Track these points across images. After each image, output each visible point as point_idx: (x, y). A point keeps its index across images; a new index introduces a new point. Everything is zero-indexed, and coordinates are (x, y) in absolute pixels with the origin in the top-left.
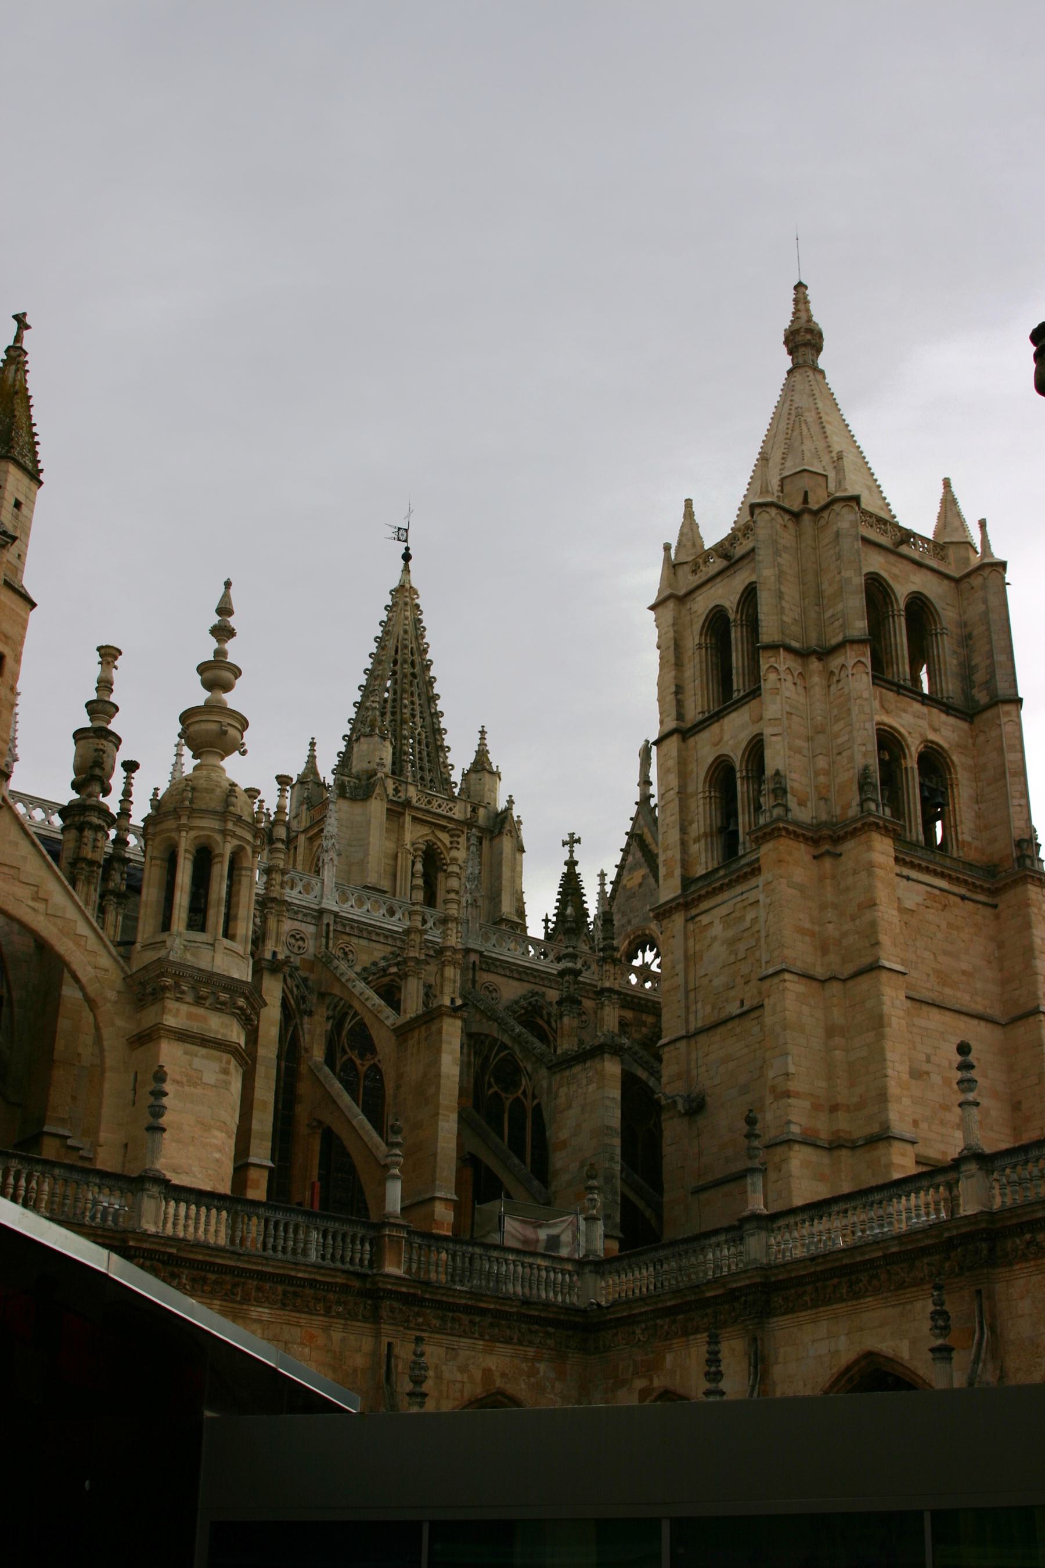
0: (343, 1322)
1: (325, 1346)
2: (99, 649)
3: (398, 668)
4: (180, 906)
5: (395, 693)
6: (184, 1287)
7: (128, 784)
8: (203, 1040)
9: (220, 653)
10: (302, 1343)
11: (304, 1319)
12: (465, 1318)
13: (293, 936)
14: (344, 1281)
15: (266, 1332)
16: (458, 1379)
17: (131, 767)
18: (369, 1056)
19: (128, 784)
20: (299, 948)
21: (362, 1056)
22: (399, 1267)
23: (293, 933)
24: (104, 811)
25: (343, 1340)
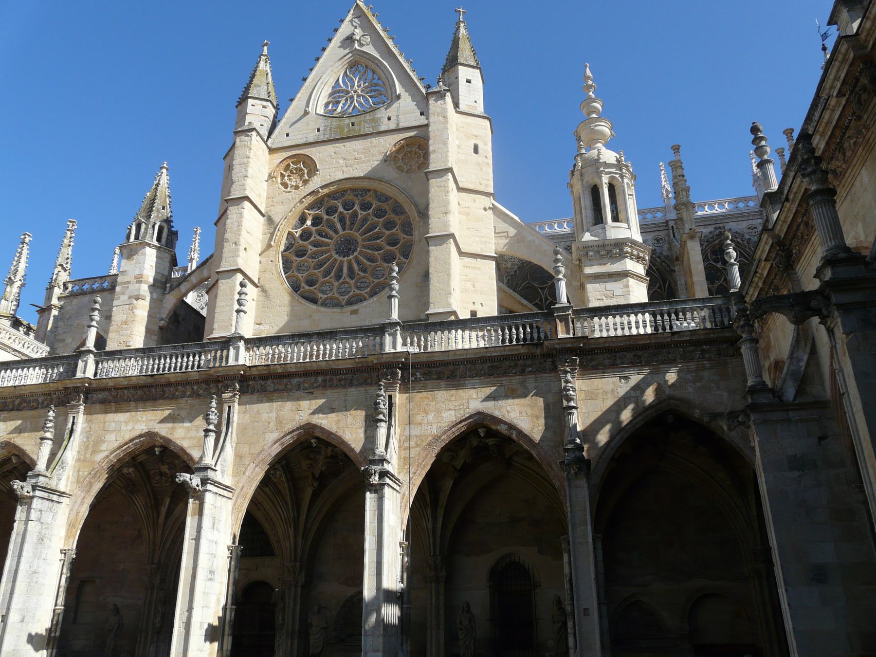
0: (533, 376)
6: (420, 380)
8: (609, 275)
12: (630, 355)
13: (749, 228)
14: (526, 351)
15: (479, 395)
16: (632, 395)
20: (755, 232)
23: (750, 227)
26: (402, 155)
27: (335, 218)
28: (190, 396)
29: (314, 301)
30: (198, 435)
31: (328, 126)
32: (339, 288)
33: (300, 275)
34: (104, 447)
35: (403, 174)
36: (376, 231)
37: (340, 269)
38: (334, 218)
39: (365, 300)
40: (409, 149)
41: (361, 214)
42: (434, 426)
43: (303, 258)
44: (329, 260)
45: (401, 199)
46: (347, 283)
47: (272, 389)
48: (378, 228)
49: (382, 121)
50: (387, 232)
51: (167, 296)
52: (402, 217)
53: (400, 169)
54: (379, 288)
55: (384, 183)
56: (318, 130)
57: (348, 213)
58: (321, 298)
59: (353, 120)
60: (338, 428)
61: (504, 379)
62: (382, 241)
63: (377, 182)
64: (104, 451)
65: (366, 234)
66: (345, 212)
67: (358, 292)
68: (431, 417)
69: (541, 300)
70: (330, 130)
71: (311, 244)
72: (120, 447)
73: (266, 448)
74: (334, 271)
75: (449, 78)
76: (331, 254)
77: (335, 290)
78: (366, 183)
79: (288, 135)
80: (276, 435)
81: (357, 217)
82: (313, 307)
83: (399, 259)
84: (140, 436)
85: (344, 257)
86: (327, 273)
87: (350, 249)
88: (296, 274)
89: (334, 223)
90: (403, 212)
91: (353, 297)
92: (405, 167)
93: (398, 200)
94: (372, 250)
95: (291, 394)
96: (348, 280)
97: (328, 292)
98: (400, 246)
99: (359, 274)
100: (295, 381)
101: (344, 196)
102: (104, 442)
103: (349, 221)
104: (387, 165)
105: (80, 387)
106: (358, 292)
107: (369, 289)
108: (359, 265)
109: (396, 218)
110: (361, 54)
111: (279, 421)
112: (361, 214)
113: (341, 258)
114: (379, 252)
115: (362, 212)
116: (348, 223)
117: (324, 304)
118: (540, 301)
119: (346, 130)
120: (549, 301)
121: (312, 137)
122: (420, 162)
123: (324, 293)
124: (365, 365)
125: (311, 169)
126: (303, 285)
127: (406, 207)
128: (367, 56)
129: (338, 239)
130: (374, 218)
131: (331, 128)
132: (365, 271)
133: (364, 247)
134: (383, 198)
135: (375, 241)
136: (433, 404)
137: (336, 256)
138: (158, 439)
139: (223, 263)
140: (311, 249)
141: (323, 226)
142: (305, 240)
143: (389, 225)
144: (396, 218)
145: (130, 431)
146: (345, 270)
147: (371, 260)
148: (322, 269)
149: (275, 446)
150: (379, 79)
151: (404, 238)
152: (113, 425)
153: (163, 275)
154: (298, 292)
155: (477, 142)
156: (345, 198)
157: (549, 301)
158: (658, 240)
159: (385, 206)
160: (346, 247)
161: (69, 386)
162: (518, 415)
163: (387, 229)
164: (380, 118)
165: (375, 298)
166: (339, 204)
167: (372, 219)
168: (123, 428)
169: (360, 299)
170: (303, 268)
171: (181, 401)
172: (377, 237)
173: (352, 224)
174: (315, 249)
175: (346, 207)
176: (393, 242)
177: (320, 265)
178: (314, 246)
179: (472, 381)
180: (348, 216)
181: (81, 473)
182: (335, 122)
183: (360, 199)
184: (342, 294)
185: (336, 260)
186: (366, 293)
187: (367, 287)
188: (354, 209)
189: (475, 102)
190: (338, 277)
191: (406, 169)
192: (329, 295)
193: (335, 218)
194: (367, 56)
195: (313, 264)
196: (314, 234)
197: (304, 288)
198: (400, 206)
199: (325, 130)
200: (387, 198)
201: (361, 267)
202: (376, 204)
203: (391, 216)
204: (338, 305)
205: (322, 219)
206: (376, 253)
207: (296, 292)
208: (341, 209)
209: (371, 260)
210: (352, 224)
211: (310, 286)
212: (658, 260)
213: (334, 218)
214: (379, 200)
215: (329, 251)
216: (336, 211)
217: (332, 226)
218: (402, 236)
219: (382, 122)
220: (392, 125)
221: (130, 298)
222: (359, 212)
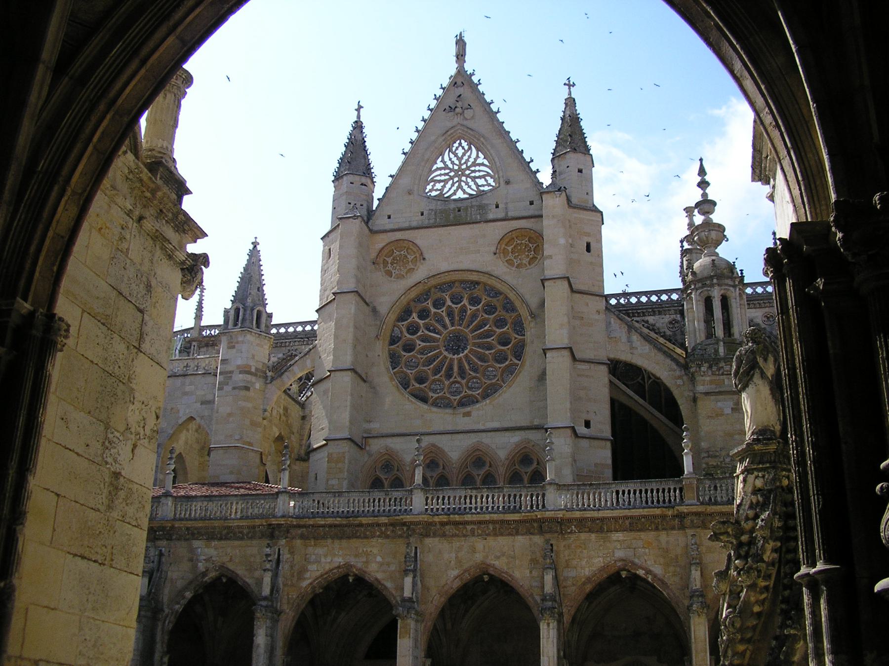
1: (658, 546)
2: (684, 210)
4: (699, 330)
9: (705, 195)
10: (643, 547)
11: (643, 535)
22: (694, 500)
25: (668, 542)
27: (443, 312)
28: (379, 536)
29: (424, 400)
30: (389, 569)
31: (432, 210)
32: (450, 386)
34: (308, 575)
35: (514, 269)
36: (486, 328)
37: (450, 368)
38: (443, 312)
39: (477, 402)
40: (519, 242)
41: (471, 309)
42: (587, 569)
44: (438, 357)
45: (512, 296)
46: (458, 383)
48: (488, 326)
49: (490, 208)
50: (498, 331)
51: (269, 386)
52: (514, 315)
53: (510, 263)
54: (491, 389)
55: (493, 278)
56: (422, 214)
57: (456, 308)
58: (432, 397)
60: (508, 568)
61: (642, 533)
62: (493, 340)
63: (487, 275)
64: (308, 579)
65: (475, 331)
66: (454, 306)
67: (470, 393)
68: (584, 563)
69: (643, 379)
71: (418, 338)
72: (322, 576)
73: (448, 582)
74: (444, 369)
75: (560, 166)
76: (441, 351)
77: (446, 390)
78: (474, 277)
79: (389, 217)
80: (455, 573)
81: (466, 312)
82: (425, 407)
83: (511, 360)
84: (339, 567)
85: (454, 355)
86: (437, 371)
87: (459, 347)
88: (405, 370)
89: (442, 316)
90: (513, 309)
91: (465, 397)
94: (483, 349)
95: (467, 538)
96: (459, 379)
97: (438, 391)
98: (512, 347)
99: (470, 374)
100: (469, 527)
101: (452, 288)
102: (308, 571)
103: (458, 315)
104: (497, 258)
105: (283, 524)
106: (470, 393)
107: (481, 390)
108: (469, 364)
110: (466, 130)
111: (459, 561)
112: (470, 309)
113: (451, 356)
114: (490, 352)
115: (471, 308)
116: (457, 318)
117: (435, 404)
118: (641, 379)
119: (452, 216)
120: (651, 380)
121: (416, 220)
123: (435, 391)
124: (529, 518)
125: (416, 257)
126: (413, 382)
127: (518, 304)
129: (447, 335)
130: (483, 315)
131: (435, 213)
132: (476, 370)
133: (474, 344)
134: (495, 293)
135: (485, 340)
136: (585, 551)
137: (446, 353)
138: (354, 570)
140: (420, 344)
141: (431, 320)
142: (413, 334)
143: (501, 323)
145: (329, 563)
146: (456, 369)
147: (482, 358)
148: (432, 366)
149: (456, 581)
151: (516, 338)
152: (314, 557)
153: (264, 363)
154: (408, 390)
155: (589, 240)
156: (453, 290)
157: (651, 380)
158: (768, 318)
159: (494, 301)
160: (456, 343)
161: (273, 523)
162: (653, 563)
164: (487, 205)
166: (447, 297)
167: (482, 316)
168: (323, 560)
169: (473, 401)
170: (412, 364)
171: (372, 540)
172: (488, 334)
173: (461, 319)
174: (423, 344)
175: (454, 300)
176: (504, 342)
177: (430, 361)
178: (423, 341)
179: (617, 535)
180: (456, 311)
181: (290, 596)
183: (469, 292)
184: (453, 393)
185: (445, 357)
186: (478, 394)
187: (478, 388)
188: (462, 303)
189: (587, 194)
190: (449, 376)
191: (516, 264)
192: (440, 394)
193: (443, 312)
194: (471, 133)
195: (422, 361)
196: (422, 328)
197: (413, 385)
198: (510, 302)
199: (429, 214)
200: (498, 293)
201: (471, 366)
202: (485, 299)
203: (500, 313)
204: (448, 405)
205: (429, 311)
206: (487, 352)
207: (405, 389)
208: (449, 303)
209: (482, 358)
210: (461, 319)
211: (420, 384)
212: (768, 340)
213: (443, 312)
214: (489, 295)
215: (438, 347)
216: (444, 304)
217: (440, 320)
219: (490, 210)
220: (501, 215)
221: (234, 388)
222: (469, 307)
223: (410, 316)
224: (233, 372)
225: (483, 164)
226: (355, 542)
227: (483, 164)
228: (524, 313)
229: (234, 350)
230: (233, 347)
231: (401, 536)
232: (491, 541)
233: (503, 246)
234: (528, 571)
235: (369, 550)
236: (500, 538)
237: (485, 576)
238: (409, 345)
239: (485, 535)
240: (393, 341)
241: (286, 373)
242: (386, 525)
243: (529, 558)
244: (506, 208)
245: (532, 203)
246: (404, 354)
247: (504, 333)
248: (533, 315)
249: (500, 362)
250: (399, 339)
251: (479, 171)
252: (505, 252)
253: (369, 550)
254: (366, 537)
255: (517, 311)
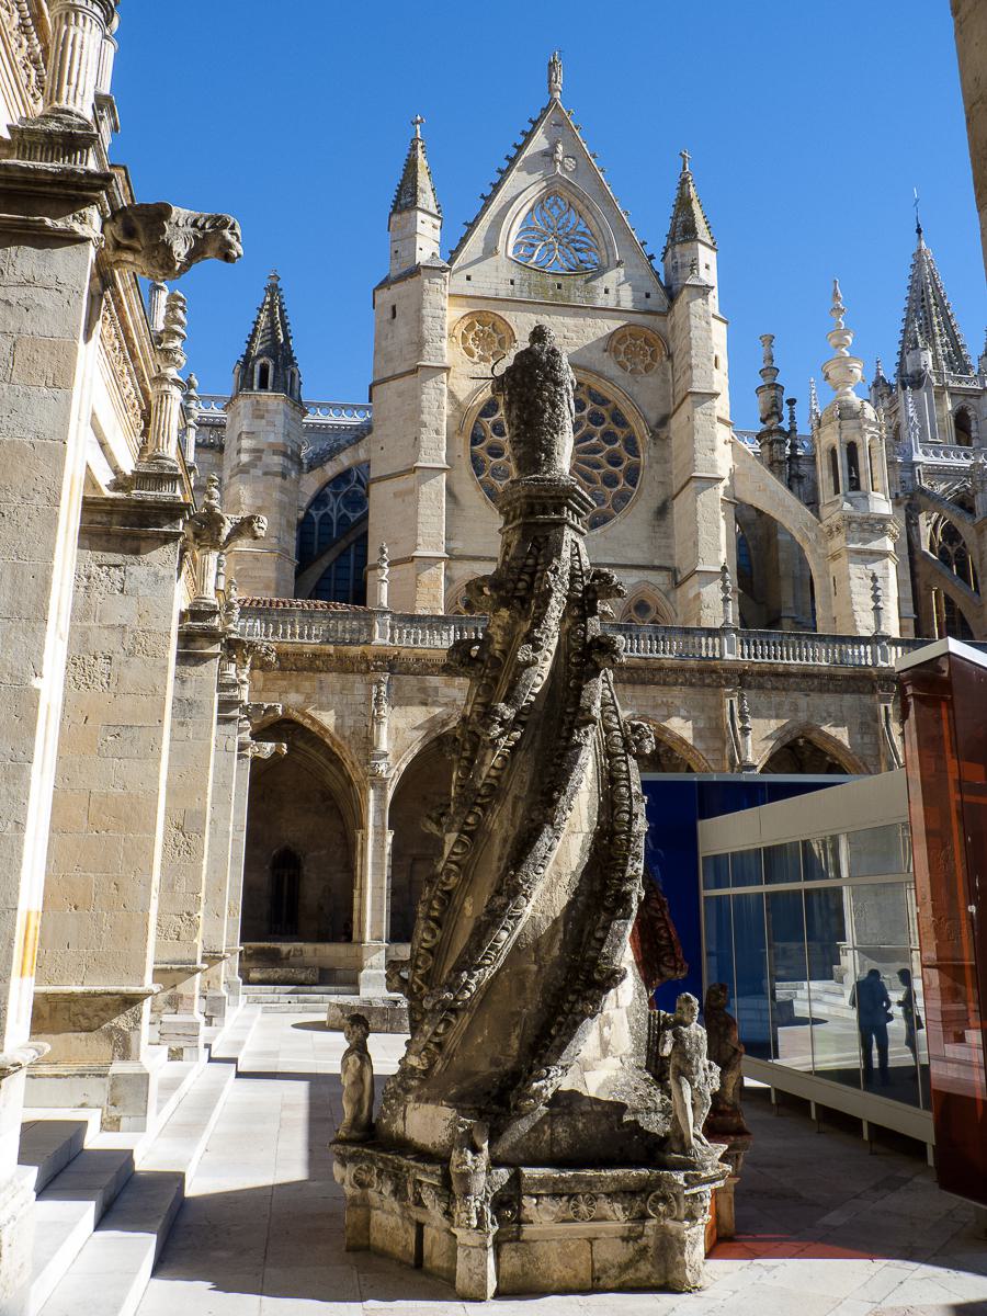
3: (925, 303)
5: (926, 319)
7: (792, 412)
17: (791, 402)
18: (955, 543)
19: (792, 412)
21: (951, 544)
24: (781, 431)
26: (625, 346)
28: (682, 684)
33: (498, 482)
40: (633, 342)
43: (500, 460)
45: (625, 408)
47: (769, 687)
50: (608, 448)
51: (305, 476)
56: (512, 283)
59: (559, 280)
70: (529, 287)
92: (628, 364)
93: (619, 406)
109: (618, 431)
110: (566, 184)
122: (647, 362)
127: (630, 419)
128: (573, 190)
139: (422, 455)
143: (609, 437)
144: (618, 431)
150: (587, 227)
159: (602, 410)
163: (607, 442)
165: (598, 531)
172: (595, 450)
182: (535, 278)
194: (573, 190)
200: (604, 401)
214: (594, 401)
218: (627, 459)
220: (612, 305)
221: (265, 474)
223: (496, 411)
224: (263, 450)
225: (584, 234)
226: (653, 690)
227: (584, 234)
228: (640, 430)
229: (264, 421)
230: (262, 417)
231: (709, 686)
232: (815, 698)
233: (614, 343)
234: (859, 736)
235: (670, 700)
236: (826, 696)
237: (801, 740)
238: (496, 449)
239: (807, 692)
240: (475, 440)
241: (330, 463)
242: (692, 670)
243: (859, 721)
244: (618, 296)
245: (648, 296)
246: (491, 459)
247: (614, 450)
248: (655, 436)
249: (610, 486)
250: (483, 439)
251: (583, 242)
252: (616, 352)
253: (670, 700)
254: (665, 684)
255: (629, 426)
